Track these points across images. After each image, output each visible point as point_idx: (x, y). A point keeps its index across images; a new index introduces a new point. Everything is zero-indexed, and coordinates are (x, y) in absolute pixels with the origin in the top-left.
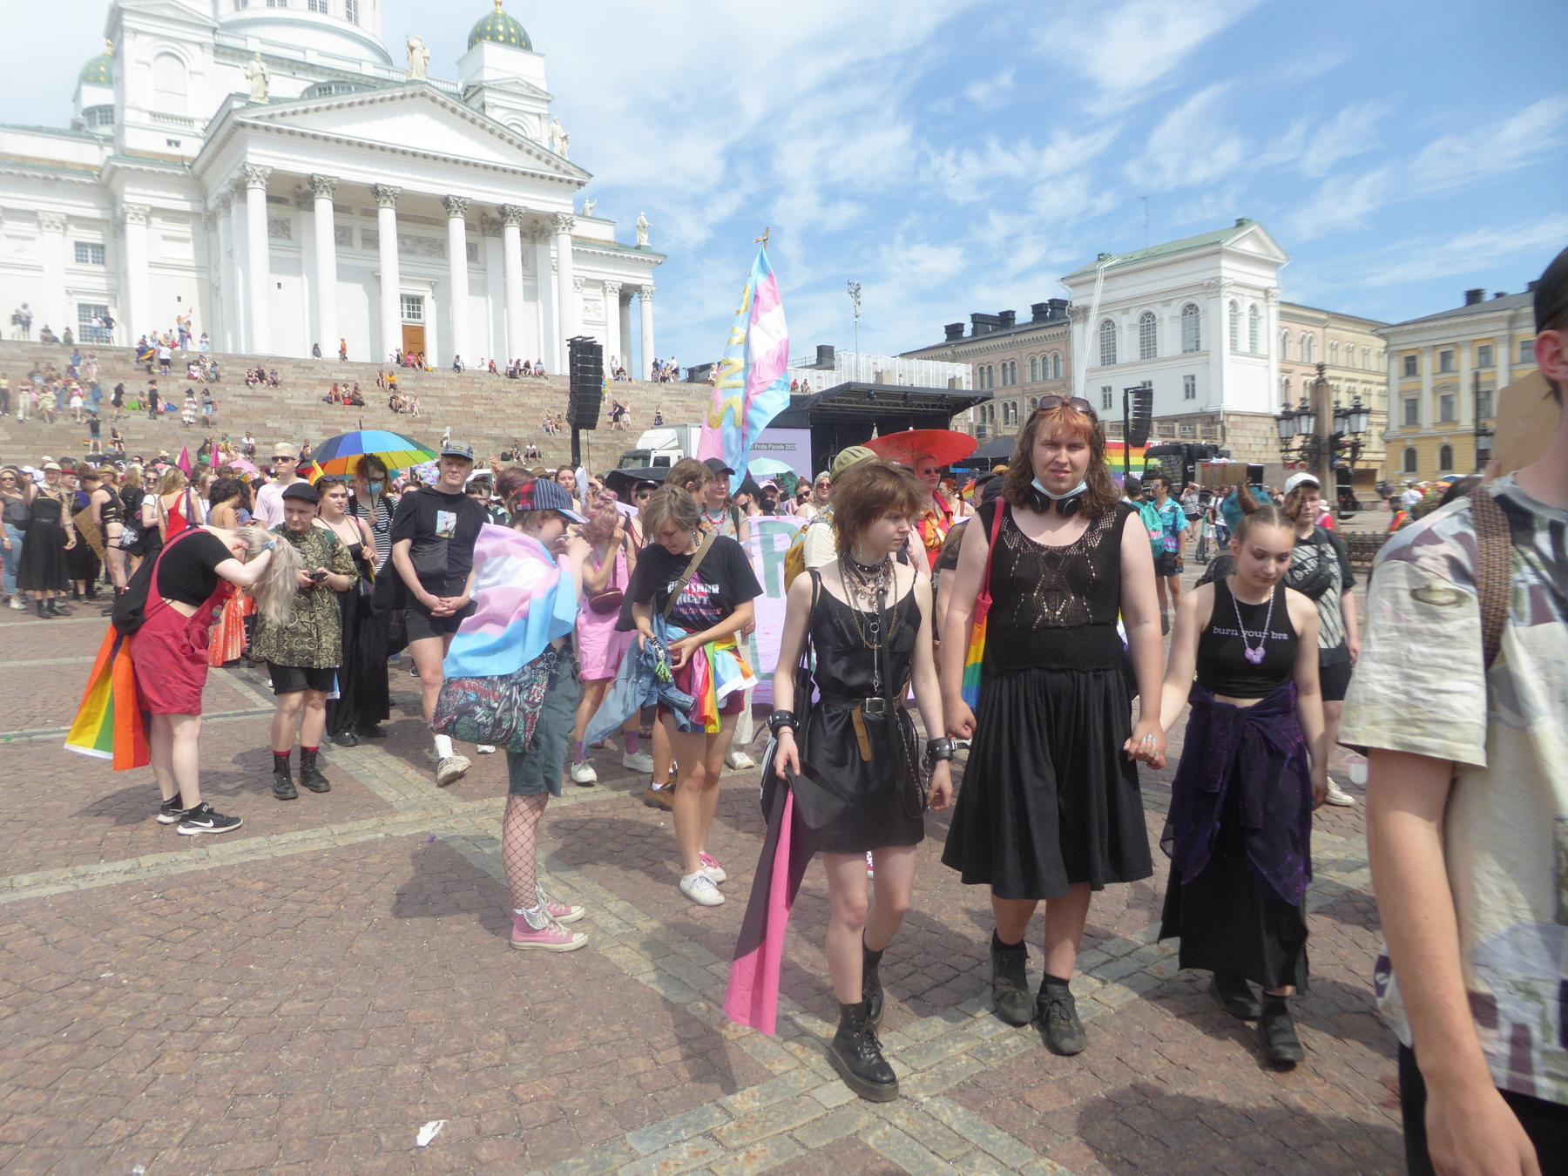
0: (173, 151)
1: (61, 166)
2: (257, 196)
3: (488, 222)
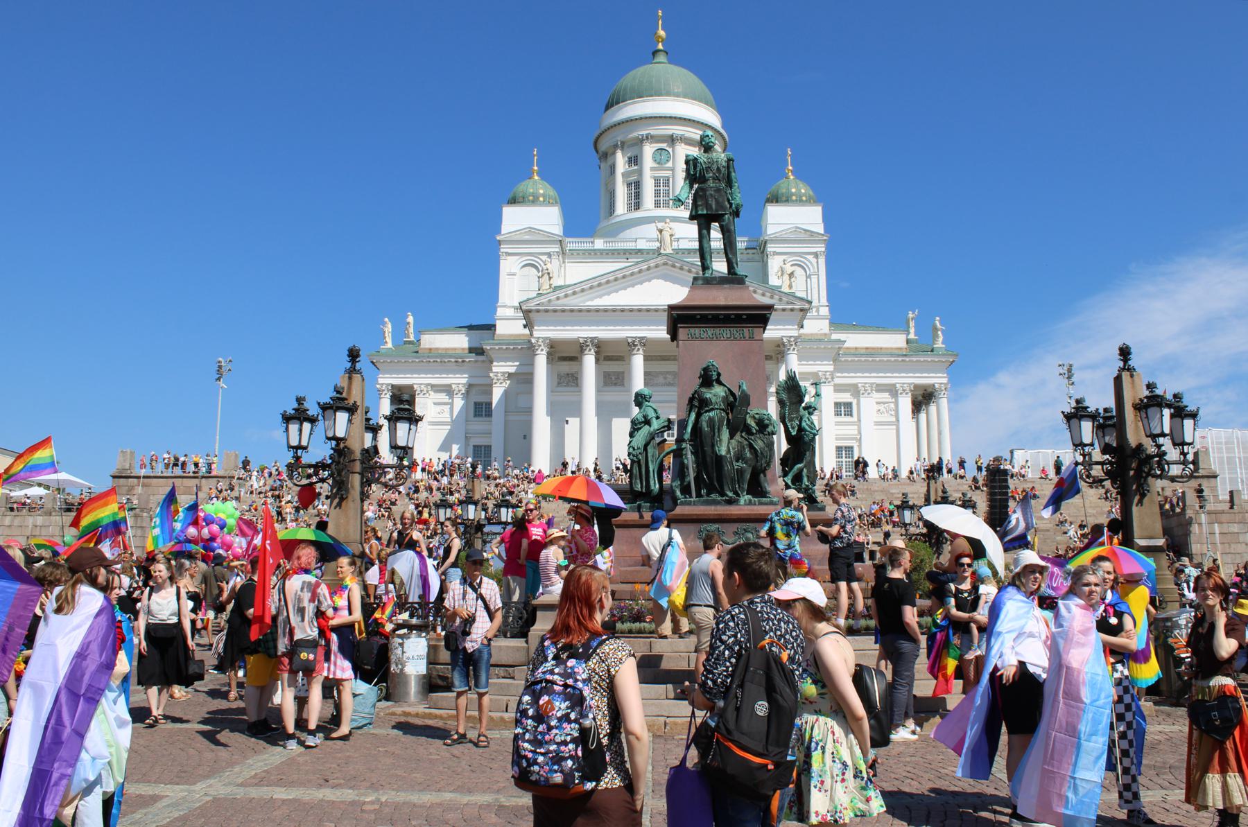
2: (541, 361)
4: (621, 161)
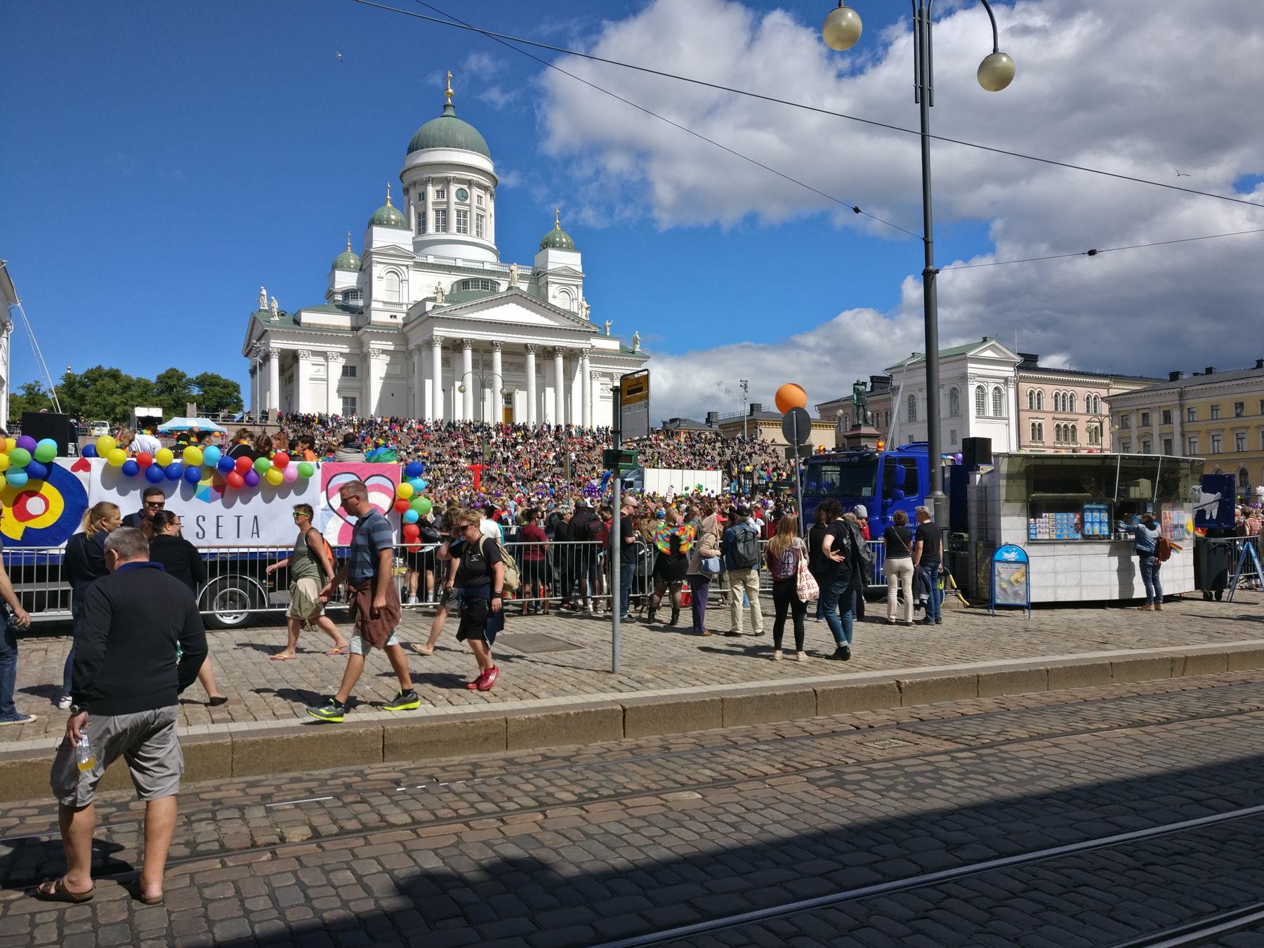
0: (393, 320)
1: (338, 329)
2: (438, 351)
3: (547, 354)
4: (431, 191)
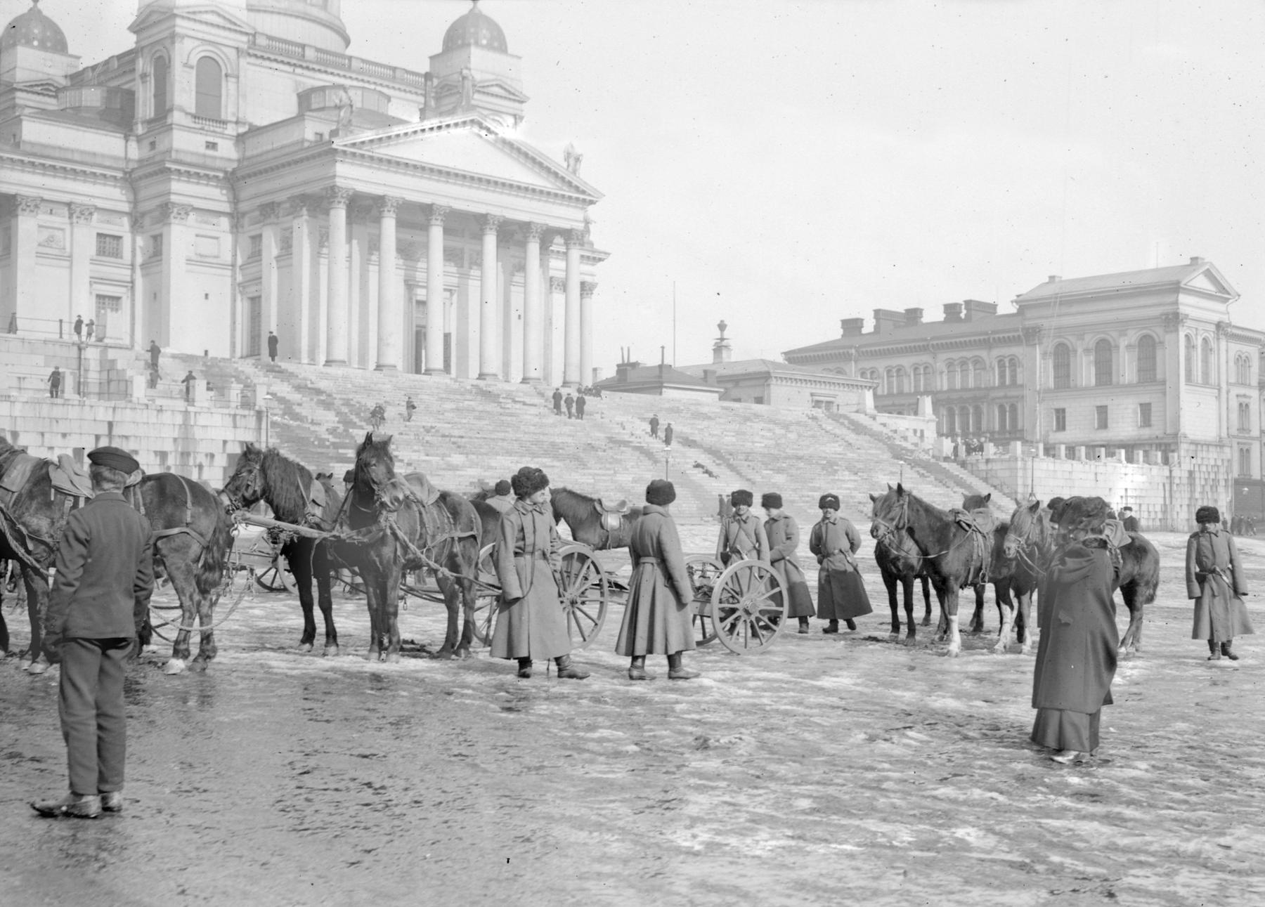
3: (513, 234)
